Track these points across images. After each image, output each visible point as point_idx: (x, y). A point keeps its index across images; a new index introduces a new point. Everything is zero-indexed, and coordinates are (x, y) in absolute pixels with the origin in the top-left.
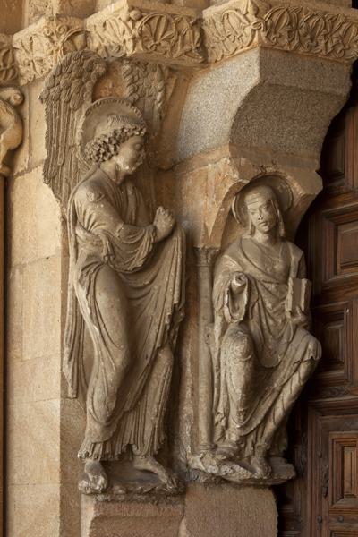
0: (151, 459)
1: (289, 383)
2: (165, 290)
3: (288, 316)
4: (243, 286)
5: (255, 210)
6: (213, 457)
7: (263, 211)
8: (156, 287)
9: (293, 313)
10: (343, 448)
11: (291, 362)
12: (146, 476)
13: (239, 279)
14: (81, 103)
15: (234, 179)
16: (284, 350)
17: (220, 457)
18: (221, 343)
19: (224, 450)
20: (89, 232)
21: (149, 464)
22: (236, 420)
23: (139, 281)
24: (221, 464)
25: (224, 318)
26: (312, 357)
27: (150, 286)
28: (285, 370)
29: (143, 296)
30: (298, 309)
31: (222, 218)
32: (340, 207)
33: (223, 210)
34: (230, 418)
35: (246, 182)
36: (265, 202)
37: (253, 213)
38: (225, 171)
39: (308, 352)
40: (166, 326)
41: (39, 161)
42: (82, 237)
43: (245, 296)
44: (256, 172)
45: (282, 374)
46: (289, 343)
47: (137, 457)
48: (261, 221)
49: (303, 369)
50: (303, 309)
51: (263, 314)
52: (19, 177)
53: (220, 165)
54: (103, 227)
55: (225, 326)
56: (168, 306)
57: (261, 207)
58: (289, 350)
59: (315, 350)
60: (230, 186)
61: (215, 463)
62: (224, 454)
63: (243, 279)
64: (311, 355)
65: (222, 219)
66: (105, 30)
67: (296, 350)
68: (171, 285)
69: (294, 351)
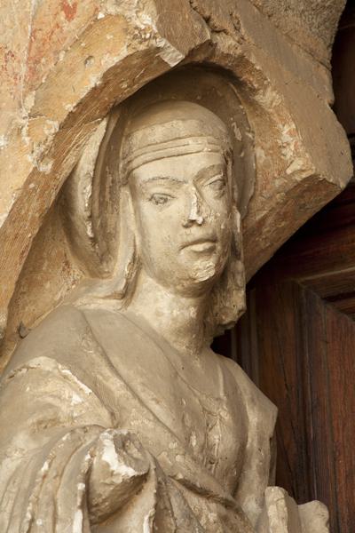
5: (177, 183)
7: (210, 193)
31: (35, 204)
33: (47, 167)
36: (217, 160)
37: (163, 200)
48: (196, 232)
57: (200, 176)
65: (34, 209)
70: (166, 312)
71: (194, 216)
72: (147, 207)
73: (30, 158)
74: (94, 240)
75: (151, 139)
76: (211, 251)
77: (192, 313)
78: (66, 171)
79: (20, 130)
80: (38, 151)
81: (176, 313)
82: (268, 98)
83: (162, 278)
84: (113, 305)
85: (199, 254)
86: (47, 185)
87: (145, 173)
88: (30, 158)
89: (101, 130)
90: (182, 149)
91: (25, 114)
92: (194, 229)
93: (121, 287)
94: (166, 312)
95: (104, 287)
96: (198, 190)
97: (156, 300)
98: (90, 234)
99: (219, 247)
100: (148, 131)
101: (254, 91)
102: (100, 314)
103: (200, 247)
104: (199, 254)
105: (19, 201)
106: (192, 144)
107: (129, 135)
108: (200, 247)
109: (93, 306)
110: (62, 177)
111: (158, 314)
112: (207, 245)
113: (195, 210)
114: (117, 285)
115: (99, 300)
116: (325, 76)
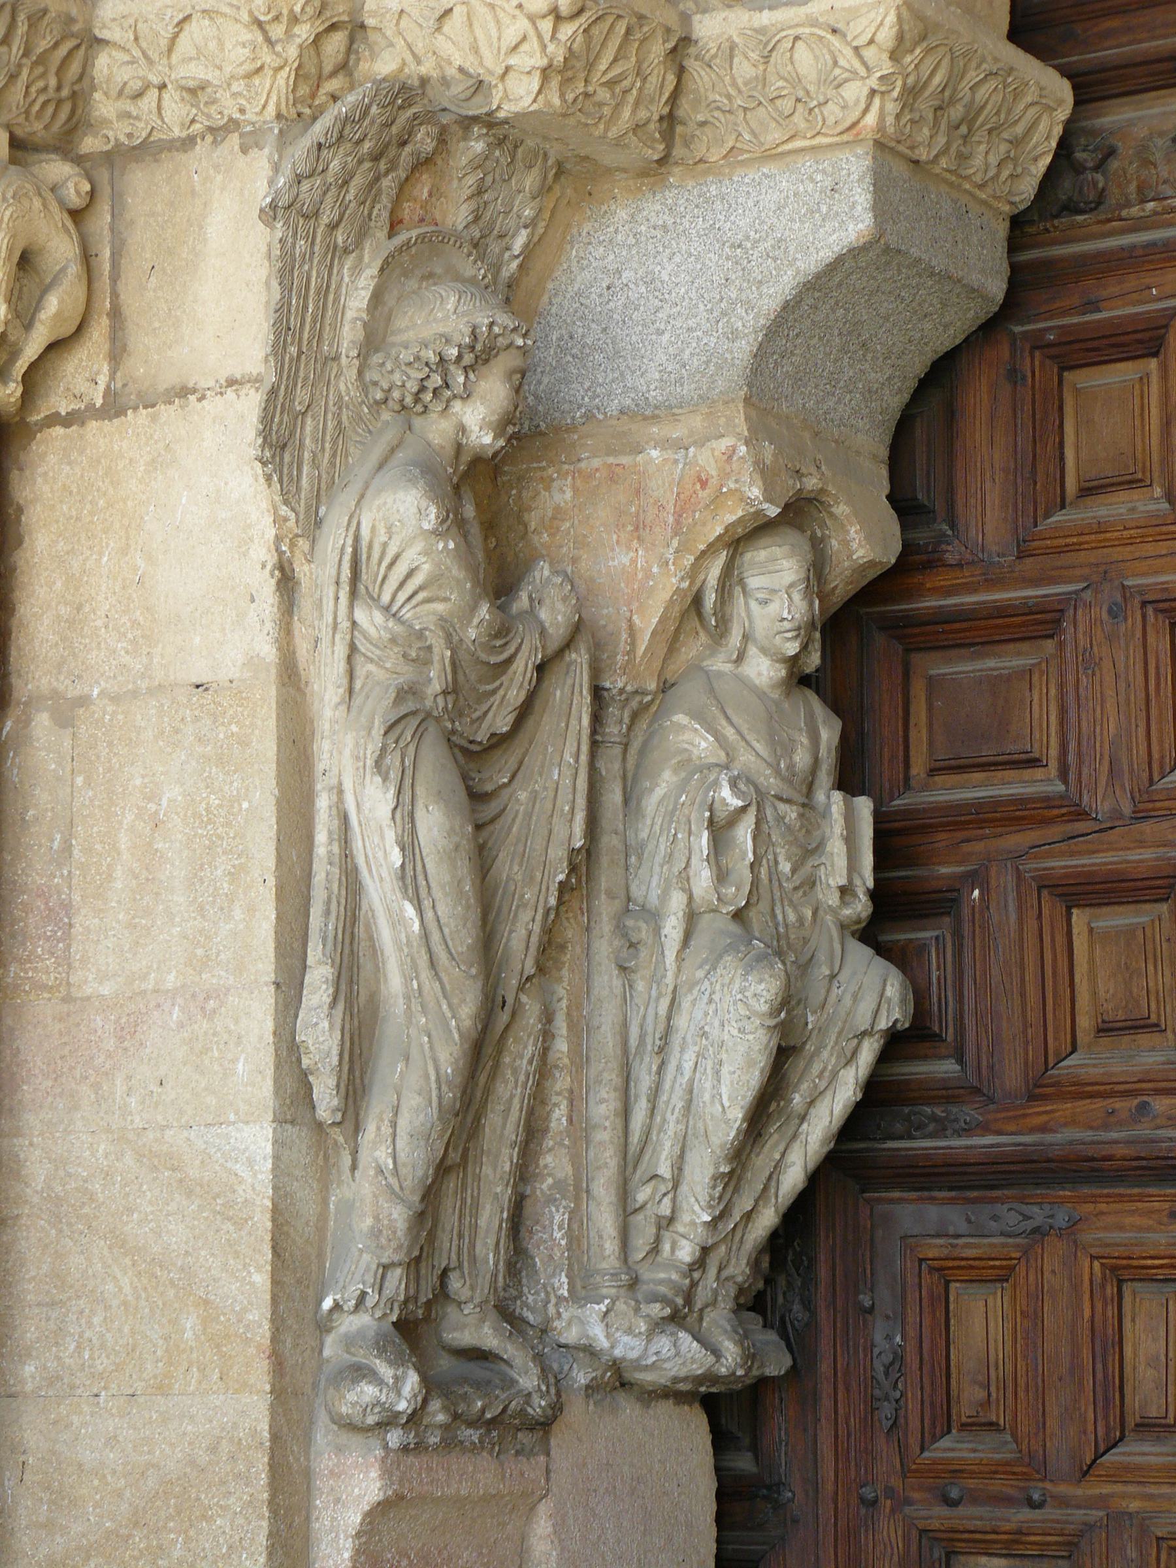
0: (493, 1315)
1: (829, 1094)
2: (549, 806)
3: (833, 899)
4: (744, 809)
5: (774, 591)
6: (637, 1310)
7: (797, 597)
8: (523, 796)
9: (845, 891)
10: (947, 1282)
11: (840, 1033)
12: (475, 1370)
13: (733, 784)
14: (362, 234)
15: (749, 502)
16: (822, 998)
17: (657, 1310)
18: (679, 969)
19: (662, 1289)
20: (400, 621)
21: (487, 1329)
22: (704, 1197)
23: (485, 775)
24: (658, 1326)
25: (691, 898)
26: (896, 1021)
27: (509, 790)
28: (825, 1054)
29: (492, 820)
30: (857, 882)
31: (677, 608)
32: (931, 603)
33: (685, 585)
34: (684, 1188)
35: (773, 511)
36: (803, 575)
37: (765, 602)
38: (724, 475)
39: (884, 1006)
40: (547, 912)
41: (161, 388)
42: (372, 632)
43: (744, 833)
44: (788, 487)
45: (816, 1068)
46: (833, 977)
47: (451, 1310)
48: (787, 625)
49: (868, 1053)
50: (870, 883)
51: (777, 894)
52: (59, 431)
53: (707, 459)
54: (440, 607)
55: (691, 918)
56: (558, 853)
57: (791, 585)
58: (833, 998)
59: (903, 1001)
60: (731, 518)
61: (643, 1327)
62: (664, 1300)
63: (742, 786)
64: (897, 1014)
66: (438, 29)
67: (855, 998)
68: (564, 795)
69: (848, 1001)
70: (765, 673)
71: (785, 615)
72: (753, 605)
73: (674, 580)
74: (716, 627)
75: (757, 559)
76: (797, 636)
77: (783, 673)
78: (698, 584)
79: (667, 563)
80: (679, 575)
81: (772, 673)
82: (841, 509)
83: (764, 651)
84: (727, 668)
85: (789, 639)
86: (686, 595)
87: (753, 582)
88: (674, 580)
89: (723, 556)
90: (777, 567)
91: (672, 551)
92: (785, 623)
93: (735, 657)
94: (765, 673)
95: (722, 656)
96: (789, 597)
97: (758, 665)
98: (713, 623)
99: (802, 632)
100: (755, 553)
101: (830, 505)
102: (720, 674)
103: (789, 635)
104: (789, 639)
105: (666, 608)
106: (785, 564)
107: (741, 554)
108: (789, 635)
109: (714, 668)
110: (695, 589)
111: (760, 674)
112: (794, 633)
113: (786, 611)
114: (731, 655)
115: (720, 664)
116: (884, 472)
